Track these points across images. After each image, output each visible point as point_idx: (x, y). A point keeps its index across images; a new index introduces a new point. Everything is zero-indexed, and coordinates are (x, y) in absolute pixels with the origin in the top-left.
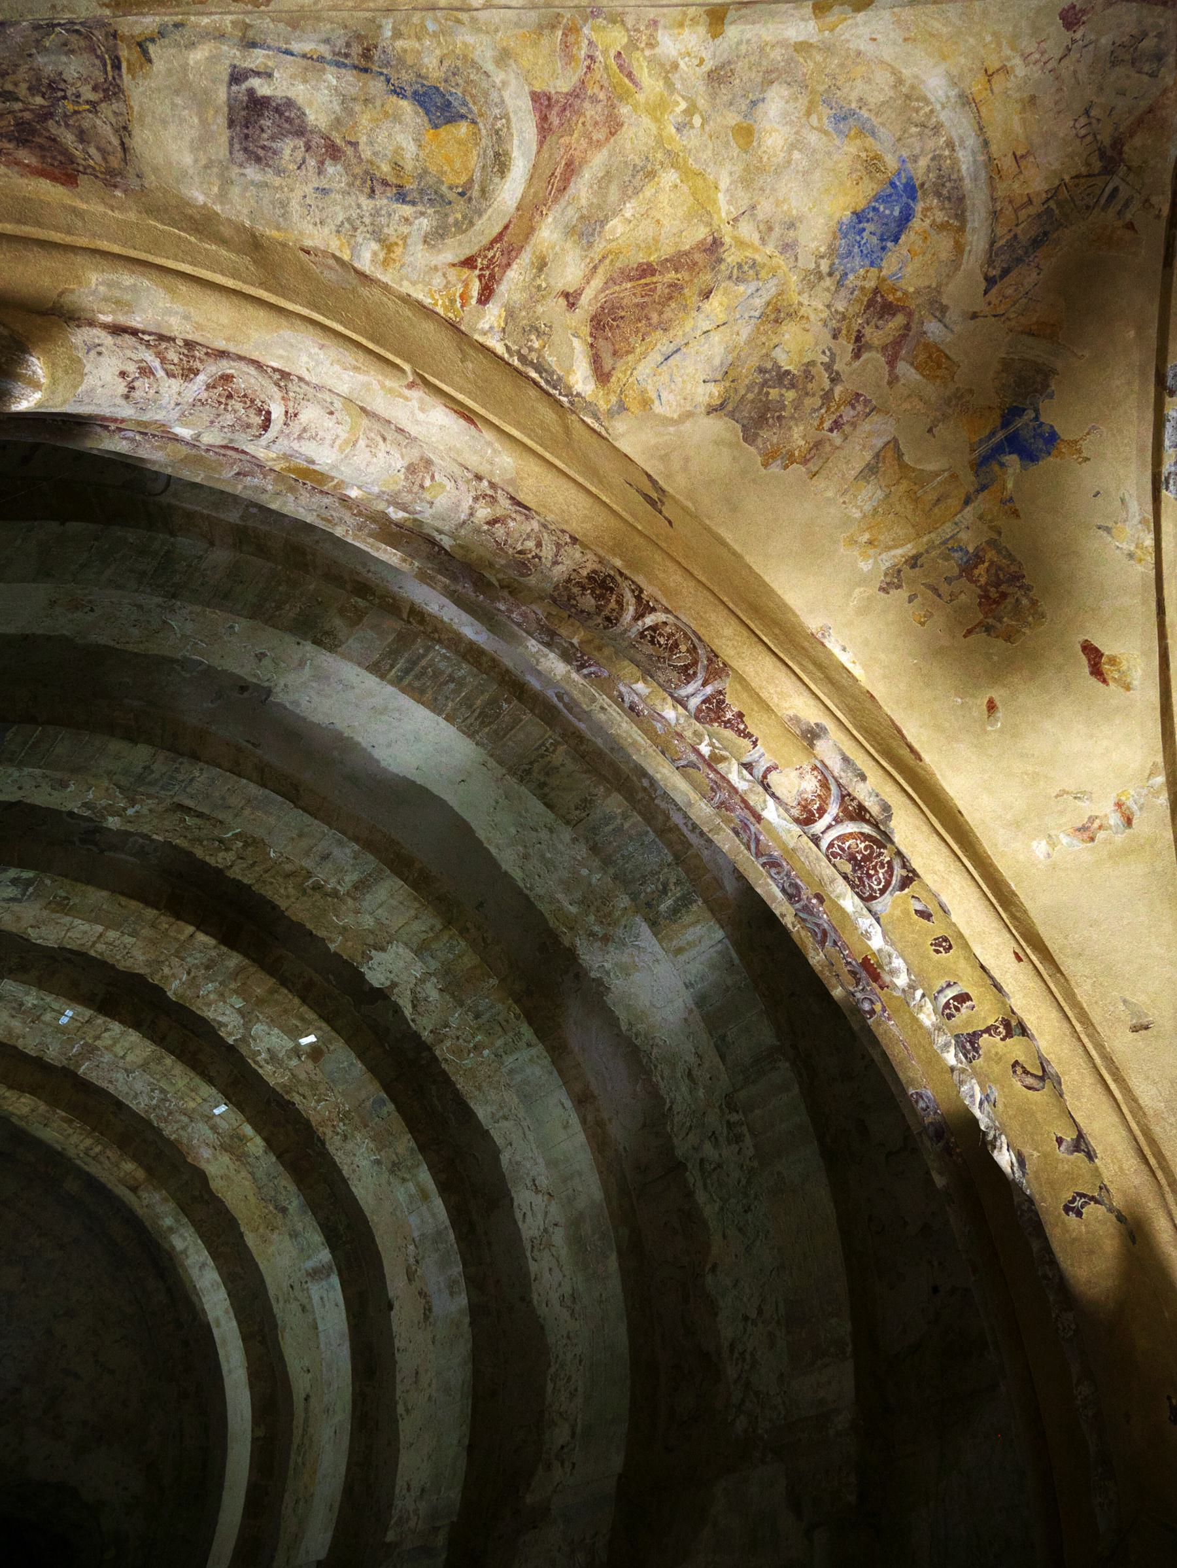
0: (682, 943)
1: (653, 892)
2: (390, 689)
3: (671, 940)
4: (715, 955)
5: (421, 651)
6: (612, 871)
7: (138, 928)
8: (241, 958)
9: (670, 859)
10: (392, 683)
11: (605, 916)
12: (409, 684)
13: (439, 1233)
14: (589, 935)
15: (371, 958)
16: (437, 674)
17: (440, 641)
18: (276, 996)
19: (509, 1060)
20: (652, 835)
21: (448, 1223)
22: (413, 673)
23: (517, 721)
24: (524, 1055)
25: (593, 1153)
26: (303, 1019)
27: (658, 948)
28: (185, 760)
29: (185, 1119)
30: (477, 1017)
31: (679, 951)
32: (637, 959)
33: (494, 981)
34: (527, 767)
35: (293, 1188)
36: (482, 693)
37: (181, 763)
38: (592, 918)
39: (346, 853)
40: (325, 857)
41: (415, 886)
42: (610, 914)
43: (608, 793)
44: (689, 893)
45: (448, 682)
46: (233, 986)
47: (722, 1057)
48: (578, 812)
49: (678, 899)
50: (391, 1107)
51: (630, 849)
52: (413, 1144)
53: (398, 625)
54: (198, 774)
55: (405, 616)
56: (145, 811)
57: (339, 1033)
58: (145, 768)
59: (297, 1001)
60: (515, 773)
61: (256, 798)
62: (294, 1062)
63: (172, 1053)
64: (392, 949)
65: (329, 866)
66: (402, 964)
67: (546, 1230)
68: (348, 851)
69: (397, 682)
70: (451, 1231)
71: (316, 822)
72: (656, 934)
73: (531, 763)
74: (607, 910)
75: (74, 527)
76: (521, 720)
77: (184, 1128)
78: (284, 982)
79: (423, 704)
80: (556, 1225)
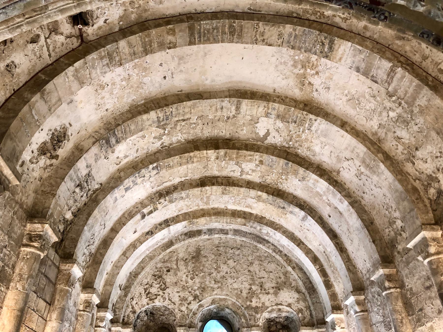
0: (340, 56)
1: (320, 47)
2: (202, 46)
3: (335, 58)
4: (353, 52)
5: (199, 27)
6: (303, 50)
7: (192, 160)
8: (223, 150)
9: (318, 32)
10: (198, 44)
11: (312, 67)
12: (204, 41)
13: (328, 189)
14: (312, 76)
15: (257, 127)
16: (208, 31)
17: (202, 20)
18: (239, 154)
19: (313, 128)
20: (307, 29)
21: (328, 185)
22: (202, 36)
23: (241, 26)
24: (316, 124)
25: (356, 139)
26: (251, 155)
27: (335, 64)
28: (165, 108)
29: (244, 200)
30: (295, 122)
31: (340, 59)
32: (331, 72)
33: (293, 109)
34: (255, 38)
35: (282, 201)
36: (225, 26)
37: (165, 110)
38: (308, 70)
39: (226, 103)
40: (222, 108)
41: (252, 98)
42: (313, 65)
43: (284, 27)
44: (331, 38)
45: (213, 31)
46: (227, 159)
47: (376, 82)
48: (280, 40)
49: (329, 43)
50: (290, 163)
51: (304, 39)
52: (303, 169)
53: (186, 24)
54: (171, 110)
55: (186, 20)
56: (169, 129)
57: (262, 153)
58: (157, 118)
59: (245, 152)
60: (253, 43)
61: (192, 105)
62: (259, 168)
63: (227, 186)
64: (260, 120)
65: (224, 110)
66: (266, 123)
67: (358, 170)
68: (226, 102)
69: (200, 42)
70: (330, 186)
71: (212, 100)
72: (330, 60)
73: (255, 36)
74: (311, 64)
75: (77, 64)
76: (242, 25)
77: (245, 202)
78: (239, 149)
79: (212, 43)
80: (360, 166)
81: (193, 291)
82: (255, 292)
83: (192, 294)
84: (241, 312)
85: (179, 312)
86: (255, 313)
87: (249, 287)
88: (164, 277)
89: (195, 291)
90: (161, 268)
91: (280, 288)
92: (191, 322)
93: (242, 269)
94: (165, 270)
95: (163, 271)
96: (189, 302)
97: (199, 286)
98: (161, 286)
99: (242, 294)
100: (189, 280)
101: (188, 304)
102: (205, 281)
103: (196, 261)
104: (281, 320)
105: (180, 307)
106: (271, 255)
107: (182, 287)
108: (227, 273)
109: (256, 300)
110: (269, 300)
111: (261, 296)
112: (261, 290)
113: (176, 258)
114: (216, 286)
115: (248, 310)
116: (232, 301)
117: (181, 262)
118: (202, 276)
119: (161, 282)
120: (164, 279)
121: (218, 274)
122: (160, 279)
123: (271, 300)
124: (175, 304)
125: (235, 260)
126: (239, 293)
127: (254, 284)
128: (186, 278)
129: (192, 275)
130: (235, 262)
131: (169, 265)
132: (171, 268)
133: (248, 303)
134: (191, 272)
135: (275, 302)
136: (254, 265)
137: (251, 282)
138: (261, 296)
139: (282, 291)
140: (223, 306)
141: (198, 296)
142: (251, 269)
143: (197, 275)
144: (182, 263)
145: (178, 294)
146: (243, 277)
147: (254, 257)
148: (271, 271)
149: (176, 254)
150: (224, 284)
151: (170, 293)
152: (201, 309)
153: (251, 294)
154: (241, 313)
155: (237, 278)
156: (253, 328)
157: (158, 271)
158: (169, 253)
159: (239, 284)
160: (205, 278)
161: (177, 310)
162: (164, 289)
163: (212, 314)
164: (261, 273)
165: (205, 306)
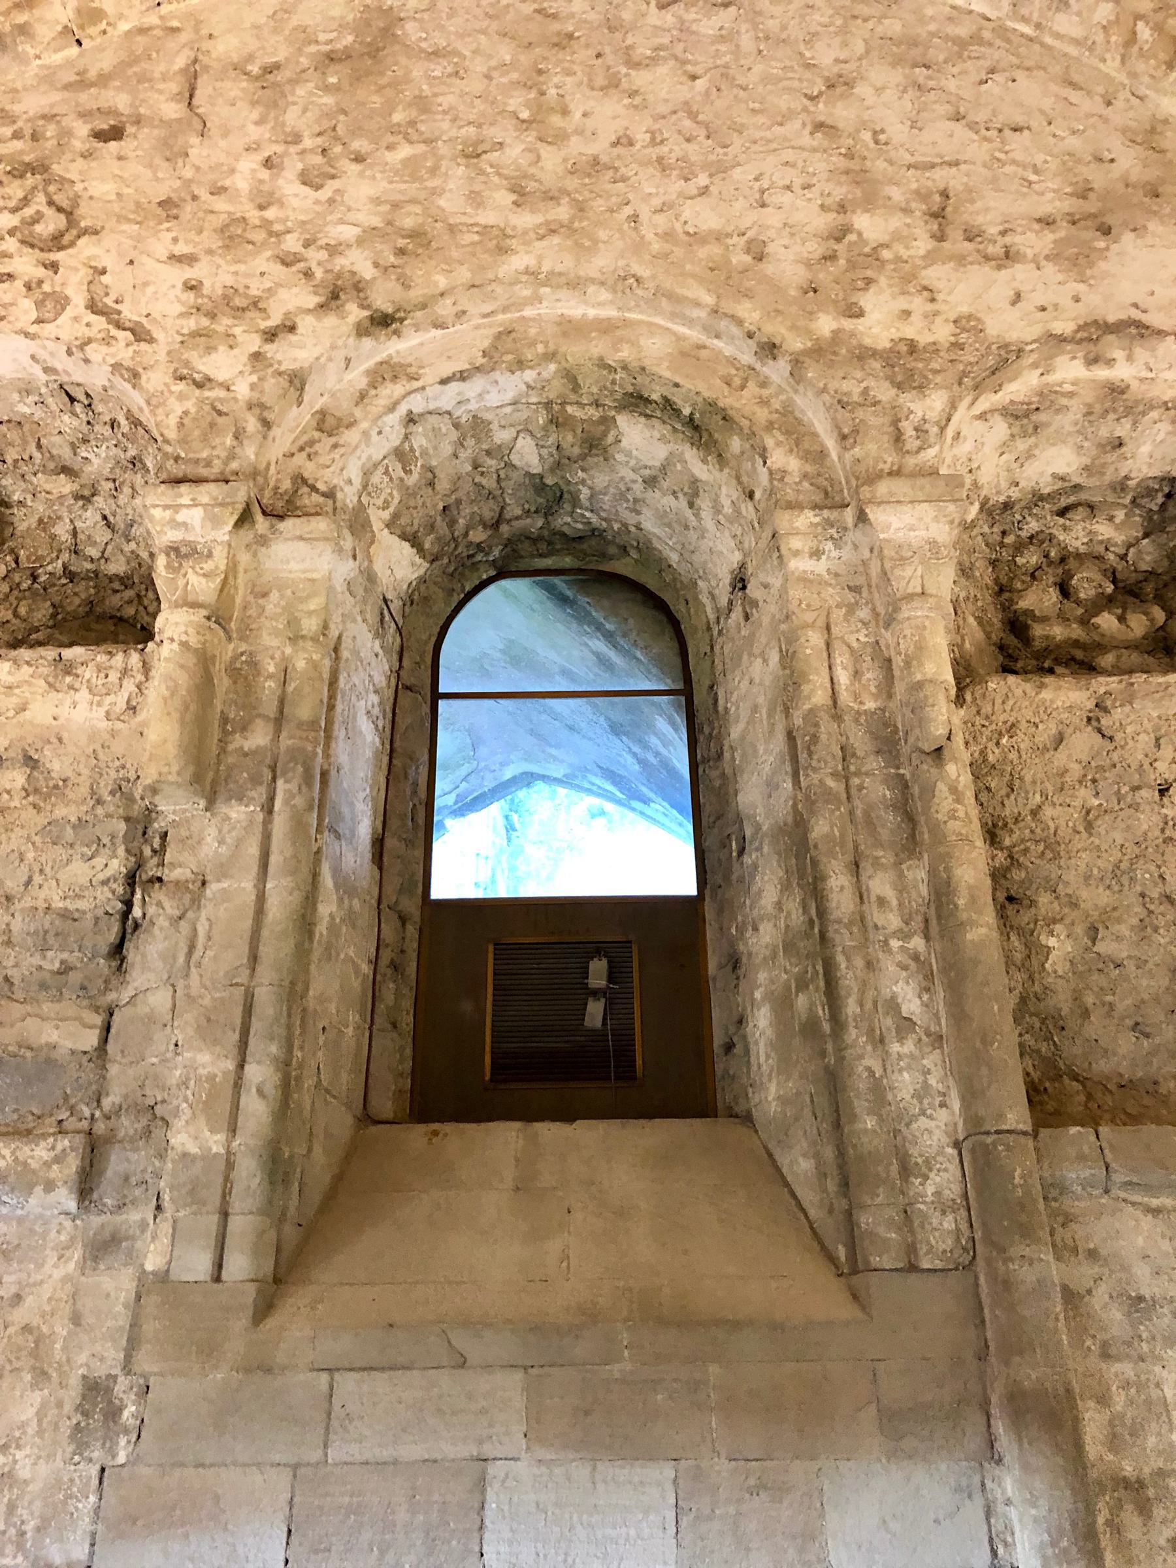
81: (323, 255)
82: (886, 254)
83: (308, 274)
84: (764, 402)
85: (180, 387)
86: (899, 386)
87: (823, 221)
88: (68, 168)
89: (333, 250)
90: (49, 117)
91: (1110, 220)
92: (300, 480)
93: (761, 119)
94: (82, 130)
95: (66, 134)
96: (274, 320)
97: (376, 221)
98: (37, 218)
99: (768, 268)
100: (289, 186)
101: (271, 336)
102: (435, 192)
103: (357, 78)
104: (1104, 530)
105: (193, 356)
106: (1002, 31)
107: (222, 230)
108: (623, 141)
109: (902, 303)
110: (1017, 298)
111: (934, 275)
112: (940, 237)
113: (181, 62)
114: (526, 220)
115: (831, 364)
116: (679, 338)
117: (228, 84)
118: (406, 162)
119: (41, 198)
120: (63, 180)
121: (546, 151)
122: (30, 180)
123: (1039, 299)
124: (140, 334)
125: (698, 70)
126: (740, 258)
127: (870, 201)
128: (265, 174)
129: (318, 159)
130: (694, 78)
131: (122, 102)
132: (138, 121)
133: (826, 324)
134: (308, 143)
135: (1082, 312)
136: (861, 90)
137: (839, 192)
138: (934, 275)
139: (1128, 238)
140: (590, 386)
141: (359, 287)
142: (842, 114)
143: (359, 159)
144: (236, 88)
145: (179, 274)
146: (771, 159)
147: (860, 48)
148: (1020, 119)
149: (184, 37)
150: (599, 205)
151: (106, 261)
152: (398, 389)
153: (852, 265)
154: (762, 415)
155: (719, 169)
156: (883, 488)
157: (17, 135)
158: (128, 33)
159: (739, 205)
160: (433, 171)
161: (156, 379)
162: (57, 242)
163: (514, 510)
164: (926, 136)
165: (430, 376)
